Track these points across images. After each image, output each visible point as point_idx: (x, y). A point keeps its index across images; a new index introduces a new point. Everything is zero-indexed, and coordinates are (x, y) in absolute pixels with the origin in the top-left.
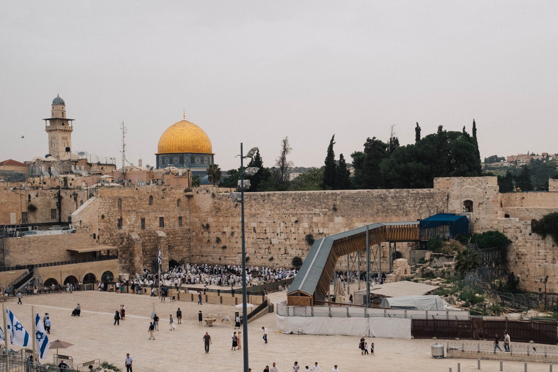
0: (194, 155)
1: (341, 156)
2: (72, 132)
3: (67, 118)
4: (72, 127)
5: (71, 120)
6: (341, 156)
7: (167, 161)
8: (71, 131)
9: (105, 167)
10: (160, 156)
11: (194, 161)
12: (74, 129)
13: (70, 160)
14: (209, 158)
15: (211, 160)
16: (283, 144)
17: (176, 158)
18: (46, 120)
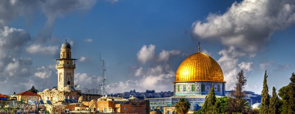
0: (204, 83)
1: (274, 89)
2: (75, 69)
3: (72, 58)
4: (75, 65)
5: (75, 59)
6: (274, 89)
7: (181, 88)
8: (75, 68)
9: (92, 97)
10: (177, 84)
11: (204, 88)
12: (76, 66)
13: (64, 91)
14: (219, 86)
15: (221, 87)
16: (239, 77)
17: (189, 86)
18: (57, 60)
